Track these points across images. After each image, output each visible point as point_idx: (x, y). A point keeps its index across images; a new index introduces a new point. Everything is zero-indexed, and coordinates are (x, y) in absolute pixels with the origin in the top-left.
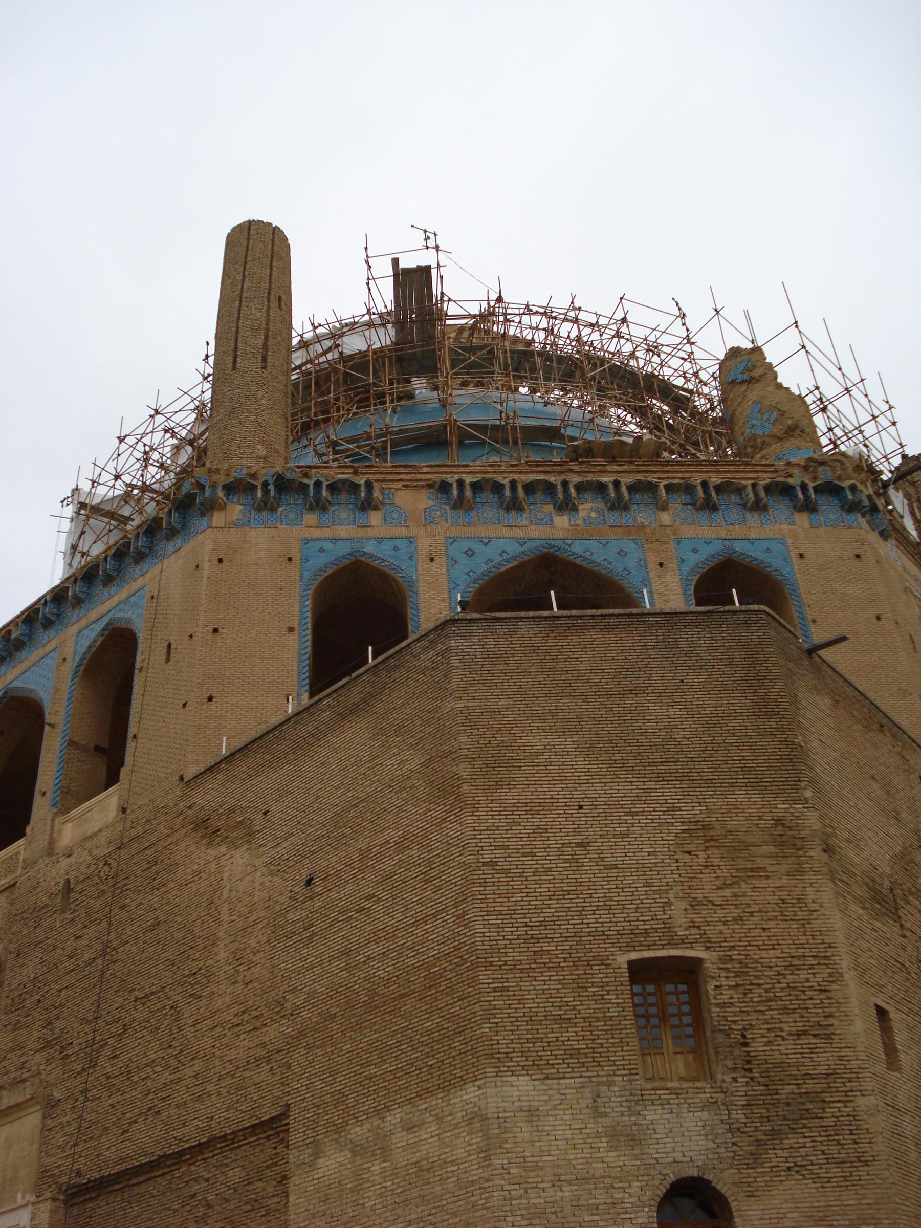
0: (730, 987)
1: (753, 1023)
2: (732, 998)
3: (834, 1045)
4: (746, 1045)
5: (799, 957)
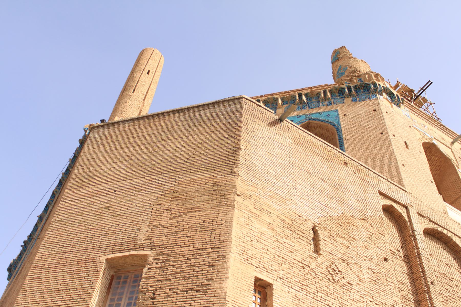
0: (156, 268)
1: (162, 286)
3: (207, 295)
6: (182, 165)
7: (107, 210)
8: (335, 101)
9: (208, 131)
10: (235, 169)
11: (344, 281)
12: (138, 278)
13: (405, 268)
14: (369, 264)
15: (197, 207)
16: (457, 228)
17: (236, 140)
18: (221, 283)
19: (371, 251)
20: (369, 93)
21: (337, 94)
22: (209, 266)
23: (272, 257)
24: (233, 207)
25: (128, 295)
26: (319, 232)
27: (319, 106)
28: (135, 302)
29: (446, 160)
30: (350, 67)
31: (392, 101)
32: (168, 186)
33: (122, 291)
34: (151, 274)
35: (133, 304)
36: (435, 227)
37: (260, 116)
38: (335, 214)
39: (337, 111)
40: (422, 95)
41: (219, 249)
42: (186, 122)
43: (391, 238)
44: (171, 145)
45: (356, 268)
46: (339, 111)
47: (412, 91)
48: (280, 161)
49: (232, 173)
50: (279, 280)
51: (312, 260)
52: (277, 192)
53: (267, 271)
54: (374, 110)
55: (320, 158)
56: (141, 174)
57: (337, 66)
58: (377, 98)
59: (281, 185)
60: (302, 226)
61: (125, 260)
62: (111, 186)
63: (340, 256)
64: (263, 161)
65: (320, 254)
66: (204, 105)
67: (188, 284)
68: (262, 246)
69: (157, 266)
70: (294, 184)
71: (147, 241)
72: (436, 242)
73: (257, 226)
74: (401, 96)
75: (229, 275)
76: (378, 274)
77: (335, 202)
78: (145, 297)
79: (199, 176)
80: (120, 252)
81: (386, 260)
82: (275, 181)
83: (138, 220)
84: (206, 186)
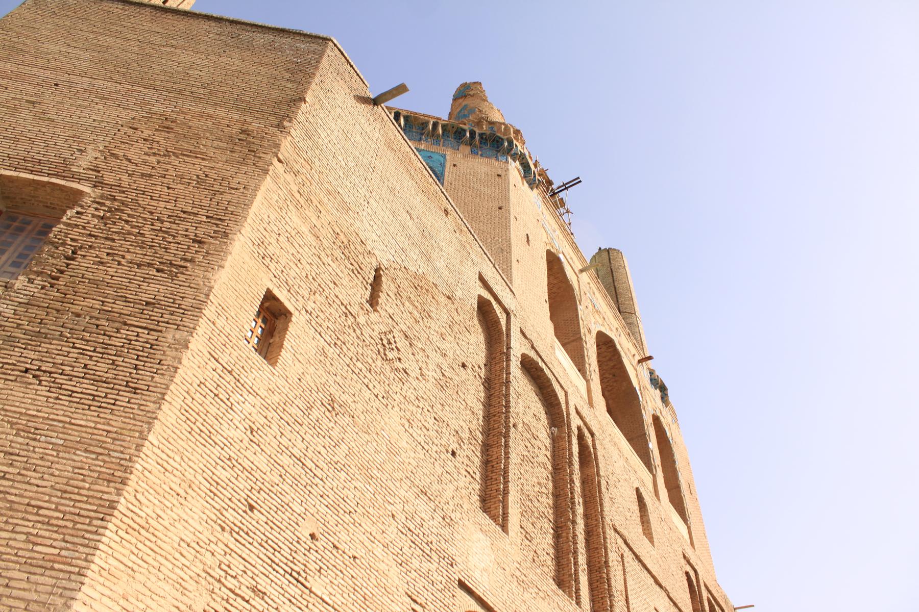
0: (93, 216)
2: (88, 223)
4: (73, 259)
5: (190, 213)
6: (194, 89)
7: (30, 106)
8: (446, 143)
9: (256, 60)
10: (286, 124)
11: (397, 364)
12: (48, 228)
13: (482, 395)
14: (441, 360)
16: (562, 374)
17: (300, 87)
18: (207, 271)
20: (498, 151)
21: (452, 135)
22: (194, 241)
24: (266, 172)
25: (20, 249)
26: (383, 279)
27: (420, 140)
29: (569, 288)
30: (480, 111)
31: (525, 177)
32: (158, 108)
33: (10, 240)
34: (80, 222)
35: (23, 266)
36: (536, 358)
37: (348, 79)
38: (412, 269)
39: (444, 156)
40: (561, 195)
41: (220, 225)
42: (222, 37)
43: (474, 346)
44: (185, 57)
45: (420, 356)
46: (448, 157)
47: (550, 183)
48: (358, 154)
49: (280, 126)
50: (303, 312)
51: (361, 312)
52: (339, 189)
53: (289, 291)
55: (414, 184)
58: (507, 162)
59: (349, 185)
60: (361, 257)
61: (36, 189)
62: (52, 76)
63: (404, 328)
64: (332, 137)
65: (376, 310)
66: (261, 27)
68: (293, 251)
70: (368, 196)
71: (91, 172)
74: (539, 175)
75: (227, 264)
76: (448, 380)
78: (54, 253)
79: (221, 112)
80: (32, 172)
81: (464, 366)
82: (341, 173)
83: (83, 136)
84: (226, 130)
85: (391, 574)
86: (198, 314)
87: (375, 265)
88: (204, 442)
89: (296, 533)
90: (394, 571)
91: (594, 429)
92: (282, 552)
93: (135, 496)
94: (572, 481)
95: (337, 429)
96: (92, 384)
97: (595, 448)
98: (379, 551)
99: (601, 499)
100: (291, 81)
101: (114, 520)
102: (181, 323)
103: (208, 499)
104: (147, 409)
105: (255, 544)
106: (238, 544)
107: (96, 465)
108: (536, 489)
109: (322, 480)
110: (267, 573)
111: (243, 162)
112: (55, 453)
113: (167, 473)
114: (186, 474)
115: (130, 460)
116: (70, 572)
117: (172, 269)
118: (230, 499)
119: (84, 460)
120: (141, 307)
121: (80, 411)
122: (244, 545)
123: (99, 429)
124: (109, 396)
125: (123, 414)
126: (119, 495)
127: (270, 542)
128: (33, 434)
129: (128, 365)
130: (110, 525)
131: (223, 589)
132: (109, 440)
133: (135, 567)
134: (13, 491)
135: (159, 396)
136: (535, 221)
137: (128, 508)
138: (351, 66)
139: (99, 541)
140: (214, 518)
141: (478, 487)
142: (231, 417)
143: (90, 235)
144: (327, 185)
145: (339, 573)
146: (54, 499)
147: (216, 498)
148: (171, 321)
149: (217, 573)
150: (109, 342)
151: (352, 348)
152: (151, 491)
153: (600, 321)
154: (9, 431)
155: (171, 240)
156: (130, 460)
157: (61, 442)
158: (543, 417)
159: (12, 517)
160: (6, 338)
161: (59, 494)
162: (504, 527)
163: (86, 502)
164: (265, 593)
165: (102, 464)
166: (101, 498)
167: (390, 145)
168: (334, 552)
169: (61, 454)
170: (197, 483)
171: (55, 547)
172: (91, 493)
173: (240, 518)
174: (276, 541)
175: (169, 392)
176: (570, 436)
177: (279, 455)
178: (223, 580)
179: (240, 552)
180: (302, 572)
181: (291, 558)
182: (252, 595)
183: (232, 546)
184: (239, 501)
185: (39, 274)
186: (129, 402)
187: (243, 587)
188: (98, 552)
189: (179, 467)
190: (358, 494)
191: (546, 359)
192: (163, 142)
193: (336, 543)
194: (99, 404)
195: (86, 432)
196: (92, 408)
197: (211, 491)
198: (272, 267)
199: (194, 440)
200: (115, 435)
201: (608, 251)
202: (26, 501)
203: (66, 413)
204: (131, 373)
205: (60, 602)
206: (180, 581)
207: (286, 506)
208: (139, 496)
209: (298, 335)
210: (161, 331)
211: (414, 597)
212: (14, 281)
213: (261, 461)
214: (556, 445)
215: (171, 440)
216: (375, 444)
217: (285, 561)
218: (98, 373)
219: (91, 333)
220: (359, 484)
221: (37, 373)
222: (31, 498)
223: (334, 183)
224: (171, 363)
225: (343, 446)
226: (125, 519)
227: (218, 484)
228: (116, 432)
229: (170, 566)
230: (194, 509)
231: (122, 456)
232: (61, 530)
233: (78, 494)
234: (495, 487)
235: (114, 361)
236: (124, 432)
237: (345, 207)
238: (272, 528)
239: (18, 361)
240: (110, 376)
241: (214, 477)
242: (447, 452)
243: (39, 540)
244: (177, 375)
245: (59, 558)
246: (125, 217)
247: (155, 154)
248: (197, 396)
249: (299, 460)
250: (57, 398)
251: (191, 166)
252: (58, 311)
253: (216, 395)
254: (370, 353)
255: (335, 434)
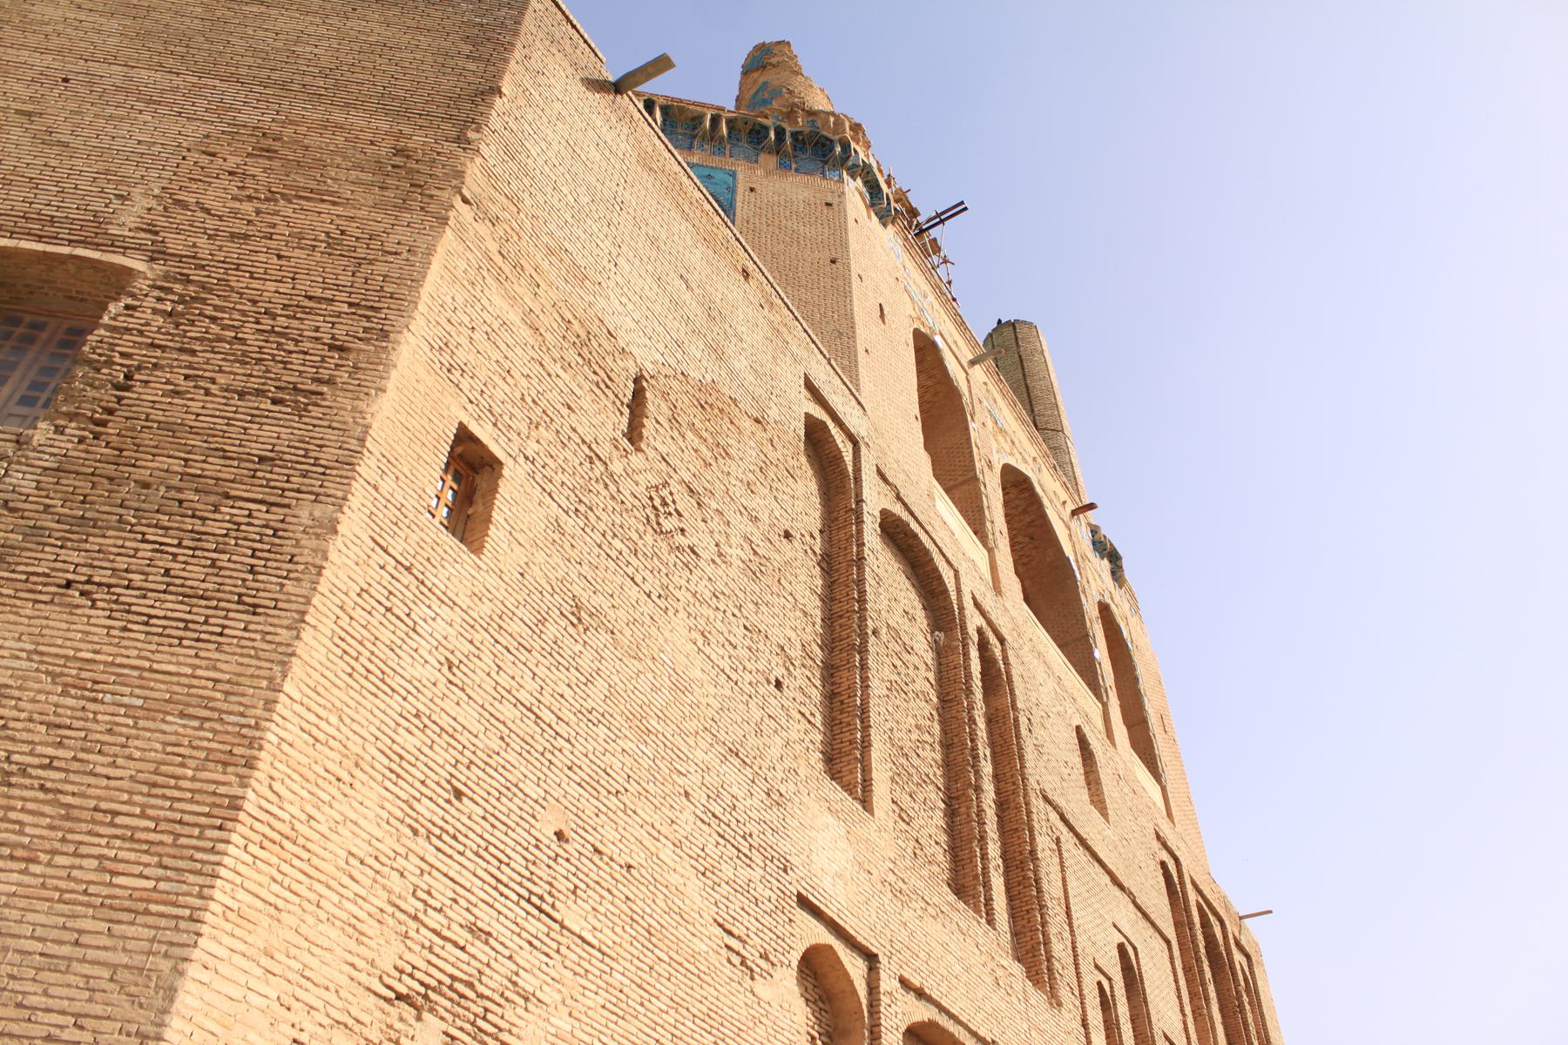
0: (155, 311)
2: (147, 324)
4: (128, 389)
5: (319, 300)
6: (308, 79)
8: (735, 150)
9: (409, 23)
10: (471, 135)
13: (819, 582)
14: (750, 528)
15: (331, 194)
16: (947, 540)
18: (358, 399)
19: (758, 500)
20: (826, 163)
22: (332, 347)
23: (519, 396)
24: (444, 221)
25: (32, 375)
26: (648, 395)
27: (690, 148)
28: (49, 400)
29: (953, 392)
30: (791, 92)
31: (872, 205)
32: (249, 116)
33: (11, 359)
34: (132, 323)
36: (905, 516)
37: (569, 50)
38: (695, 374)
39: (733, 175)
40: (934, 233)
41: (374, 317)
43: (801, 500)
46: (740, 176)
47: (913, 213)
49: (461, 140)
50: (521, 459)
51: (615, 452)
52: (567, 245)
53: (495, 425)
54: (828, 204)
56: (170, 62)
57: (755, 82)
58: (841, 180)
59: (583, 236)
60: (609, 359)
63: (687, 477)
65: (638, 450)
67: (251, 375)
68: (496, 355)
69: (159, 306)
70: (614, 253)
71: (143, 235)
72: (895, 555)
73: (497, 300)
75: (391, 385)
76: (764, 561)
77: (702, 346)
78: (94, 379)
79: (357, 119)
80: (40, 238)
81: (787, 535)
84: (370, 150)
85: (688, 891)
86: (349, 474)
87: (633, 371)
88: (374, 690)
89: (533, 831)
90: (694, 885)
91: (1004, 631)
92: (513, 864)
93: (271, 787)
94: (972, 721)
95: (588, 654)
96: (182, 603)
97: (1007, 664)
98: (667, 853)
99: (1020, 748)
100: (474, 59)
101: (239, 827)
102: (322, 490)
103: (388, 784)
104: (277, 639)
105: (469, 854)
106: (440, 855)
107: (201, 739)
108: (914, 737)
109: (568, 741)
110: (491, 901)
111: (404, 206)
112: (131, 722)
113: (318, 746)
114: (349, 744)
115: (257, 727)
116: (177, 917)
117: (298, 399)
118: (423, 782)
119: (181, 730)
120: (250, 466)
121: (166, 649)
122: (450, 857)
123: (200, 678)
124: (212, 621)
125: (239, 650)
126: (245, 786)
127: (491, 849)
128: (91, 690)
129: (238, 566)
130: (234, 837)
131: (423, 930)
132: (219, 695)
133: (280, 903)
134: (69, 788)
135: (296, 616)
136: (892, 280)
137: (260, 807)
138: (574, 27)
139: (218, 864)
140: (400, 814)
141: (819, 738)
142: (415, 646)
143: (152, 345)
144: (546, 239)
145: (605, 893)
146: (137, 798)
147: (400, 782)
148: (304, 488)
149: (412, 905)
150: (203, 529)
151: (604, 516)
152: (296, 777)
153: (1007, 447)
154: (50, 687)
155: (292, 348)
156: (257, 727)
157: (140, 702)
158: (920, 614)
159: (72, 831)
160: (28, 531)
161: (145, 789)
162: (866, 803)
163: (191, 801)
164: (489, 934)
165: (210, 736)
166: (214, 793)
167: (645, 162)
168: (596, 858)
169: (141, 723)
170: (368, 758)
171: (147, 878)
172: (198, 785)
173: (441, 813)
174: (502, 847)
175: (311, 610)
176: (965, 646)
177: (496, 703)
178: (420, 915)
179: (445, 869)
180: (546, 896)
181: (527, 874)
182: (469, 937)
183: (432, 860)
184: (438, 784)
185: (72, 417)
186: (245, 629)
187: (455, 927)
188: (219, 882)
189: (336, 734)
190: (628, 761)
191: (921, 518)
192: (262, 177)
193: (598, 844)
194: (196, 635)
195: (178, 684)
196: (185, 642)
197: (392, 771)
198: (465, 385)
199: (358, 687)
200: (227, 687)
201: (1013, 325)
202: (92, 803)
203: (143, 654)
204: (244, 580)
205: (165, 965)
206: (353, 921)
207: (514, 789)
208: (277, 786)
209: (515, 501)
210: (288, 506)
211: (728, 926)
212: (30, 432)
213: (468, 715)
214: (944, 661)
215: (319, 689)
216: (650, 676)
217: (519, 879)
218: (189, 583)
219: (171, 515)
220: (628, 745)
221: (87, 587)
222: (99, 798)
223: (558, 234)
224: (310, 560)
225: (600, 683)
226: (257, 825)
227: (401, 757)
228: (229, 682)
229: (336, 898)
230: (367, 803)
231: (243, 721)
232: (154, 849)
233: (176, 787)
234: (847, 737)
235: (214, 560)
236: (242, 680)
237: (579, 276)
238: (493, 826)
239: (53, 569)
240: (210, 586)
241: (395, 747)
242: (769, 682)
243: (121, 867)
244: (322, 580)
245: (155, 895)
246: (209, 311)
247: (250, 198)
248: (358, 614)
249: (530, 710)
250: (125, 629)
251: (314, 217)
252: (111, 479)
253: (388, 610)
254: (634, 523)
255: (586, 662)
